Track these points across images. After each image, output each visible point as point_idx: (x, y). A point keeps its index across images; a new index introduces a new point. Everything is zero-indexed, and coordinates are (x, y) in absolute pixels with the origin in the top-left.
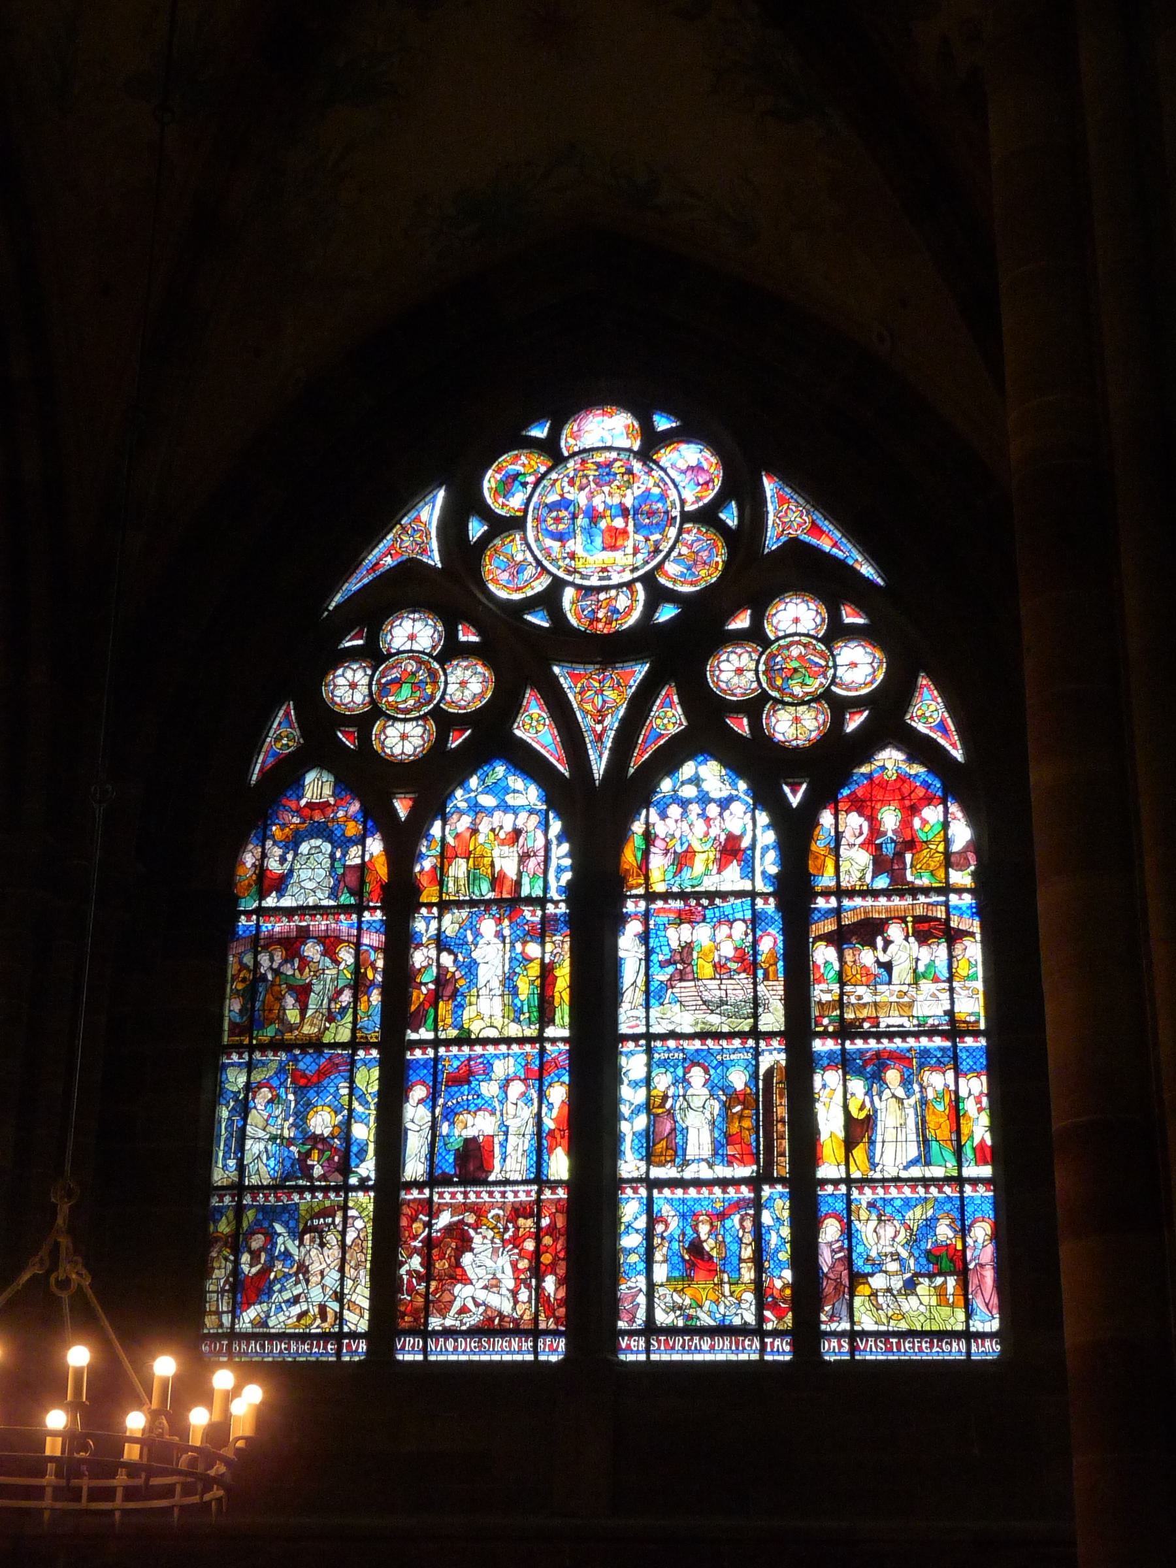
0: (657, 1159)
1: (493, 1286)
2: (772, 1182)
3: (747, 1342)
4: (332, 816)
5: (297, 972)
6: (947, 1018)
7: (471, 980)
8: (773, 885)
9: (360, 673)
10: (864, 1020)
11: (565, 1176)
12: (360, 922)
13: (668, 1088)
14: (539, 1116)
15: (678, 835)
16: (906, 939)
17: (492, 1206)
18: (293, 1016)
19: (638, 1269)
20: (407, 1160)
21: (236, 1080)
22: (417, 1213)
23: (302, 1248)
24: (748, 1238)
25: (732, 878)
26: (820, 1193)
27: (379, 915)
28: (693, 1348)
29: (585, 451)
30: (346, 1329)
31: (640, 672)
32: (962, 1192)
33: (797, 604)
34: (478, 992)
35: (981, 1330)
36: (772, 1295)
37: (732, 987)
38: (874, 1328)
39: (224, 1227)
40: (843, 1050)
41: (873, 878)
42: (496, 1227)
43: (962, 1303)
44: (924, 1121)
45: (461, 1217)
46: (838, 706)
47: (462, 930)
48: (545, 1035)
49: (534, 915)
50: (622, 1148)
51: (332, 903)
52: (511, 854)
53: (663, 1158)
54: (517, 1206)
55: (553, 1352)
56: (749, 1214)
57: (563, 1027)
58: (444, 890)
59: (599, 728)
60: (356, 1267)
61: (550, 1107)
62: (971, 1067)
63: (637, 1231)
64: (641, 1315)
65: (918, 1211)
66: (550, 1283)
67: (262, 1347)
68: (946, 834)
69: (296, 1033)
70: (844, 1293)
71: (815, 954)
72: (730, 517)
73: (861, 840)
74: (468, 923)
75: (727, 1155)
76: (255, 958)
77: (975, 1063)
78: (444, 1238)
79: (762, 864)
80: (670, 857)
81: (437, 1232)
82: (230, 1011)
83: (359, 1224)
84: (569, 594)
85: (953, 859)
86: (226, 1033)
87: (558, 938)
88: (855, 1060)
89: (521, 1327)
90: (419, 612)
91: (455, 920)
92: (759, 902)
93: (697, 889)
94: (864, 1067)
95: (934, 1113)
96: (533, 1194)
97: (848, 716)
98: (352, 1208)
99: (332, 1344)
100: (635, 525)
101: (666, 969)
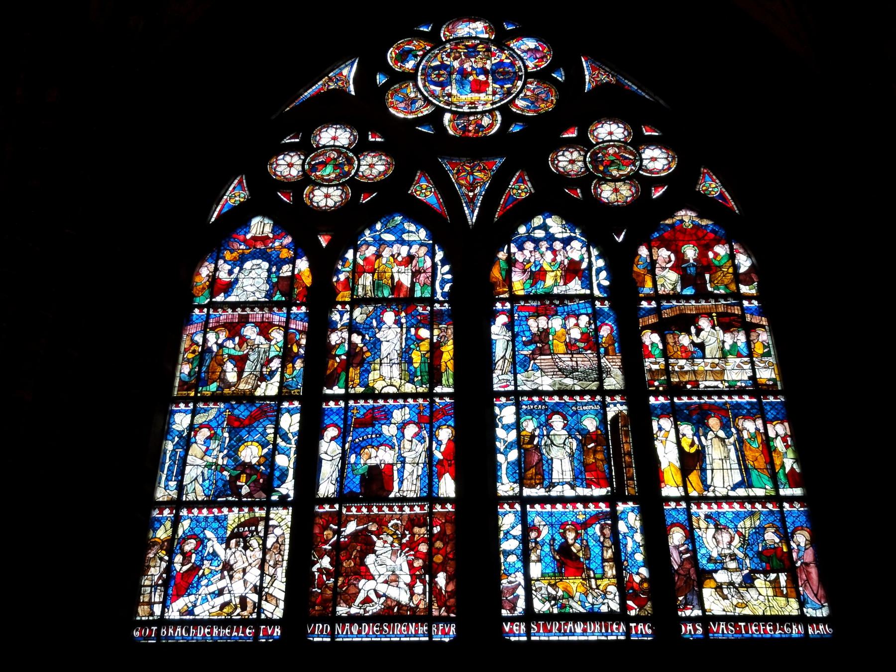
3: (615, 626)
4: (270, 245)
5: (237, 346)
11: (452, 495)
12: (289, 313)
14: (430, 452)
16: (713, 327)
18: (232, 377)
19: (516, 566)
21: (181, 421)
22: (328, 523)
24: (608, 543)
25: (575, 287)
27: (304, 309)
30: (263, 616)
32: (782, 507)
36: (632, 588)
37: (581, 359)
39: (162, 534)
41: (682, 290)
42: (395, 533)
44: (743, 456)
47: (369, 319)
49: (424, 309)
50: (499, 474)
55: (445, 634)
56: (607, 524)
58: (355, 293)
60: (275, 566)
62: (775, 416)
63: (514, 537)
65: (748, 523)
67: (188, 631)
69: (233, 388)
70: (694, 586)
72: (559, 76)
73: (669, 265)
74: (374, 314)
77: (778, 414)
79: (597, 279)
80: (527, 275)
81: (345, 538)
83: (278, 531)
85: (741, 278)
86: (176, 389)
89: (418, 614)
90: (340, 124)
92: (598, 304)
96: (426, 508)
98: (272, 519)
99: (250, 629)
100: (493, 79)
101: (529, 347)
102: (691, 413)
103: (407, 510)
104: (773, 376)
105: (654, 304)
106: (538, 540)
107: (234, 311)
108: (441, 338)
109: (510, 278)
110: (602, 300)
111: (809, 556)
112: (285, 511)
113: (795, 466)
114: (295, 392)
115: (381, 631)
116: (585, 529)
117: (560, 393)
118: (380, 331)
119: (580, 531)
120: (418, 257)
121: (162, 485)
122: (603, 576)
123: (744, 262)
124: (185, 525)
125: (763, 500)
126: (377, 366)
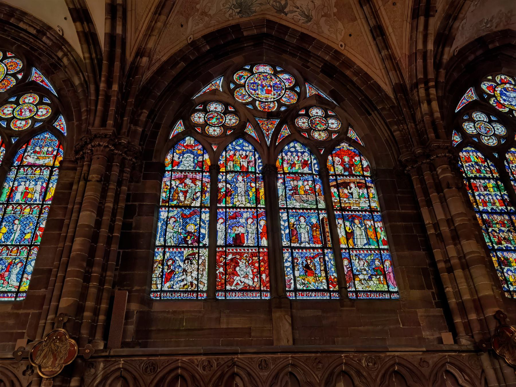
1: (246, 277)
2: (328, 248)
3: (326, 294)
10: (347, 207)
12: (202, 175)
13: (294, 222)
15: (291, 159)
16: (356, 187)
18: (182, 198)
20: (218, 239)
21: (163, 215)
22: (221, 255)
24: (322, 264)
25: (306, 170)
27: (208, 174)
32: (380, 252)
36: (331, 280)
40: (342, 214)
42: (246, 259)
44: (367, 234)
46: (330, 132)
49: (253, 176)
55: (267, 297)
57: (263, 205)
60: (203, 271)
63: (289, 261)
64: (292, 286)
65: (369, 258)
66: (264, 276)
67: (172, 295)
73: (339, 163)
79: (314, 167)
83: (203, 258)
84: (257, 102)
85: (364, 169)
86: (161, 203)
87: (260, 182)
92: (315, 177)
94: (349, 218)
102: (349, 218)
103: (250, 251)
105: (334, 178)
107: (181, 173)
110: (316, 175)
111: (390, 270)
112: (205, 251)
113: (385, 238)
114: (206, 205)
115: (243, 295)
116: (314, 259)
117: (303, 209)
121: (158, 239)
123: (365, 164)
124: (168, 255)
126: (237, 197)
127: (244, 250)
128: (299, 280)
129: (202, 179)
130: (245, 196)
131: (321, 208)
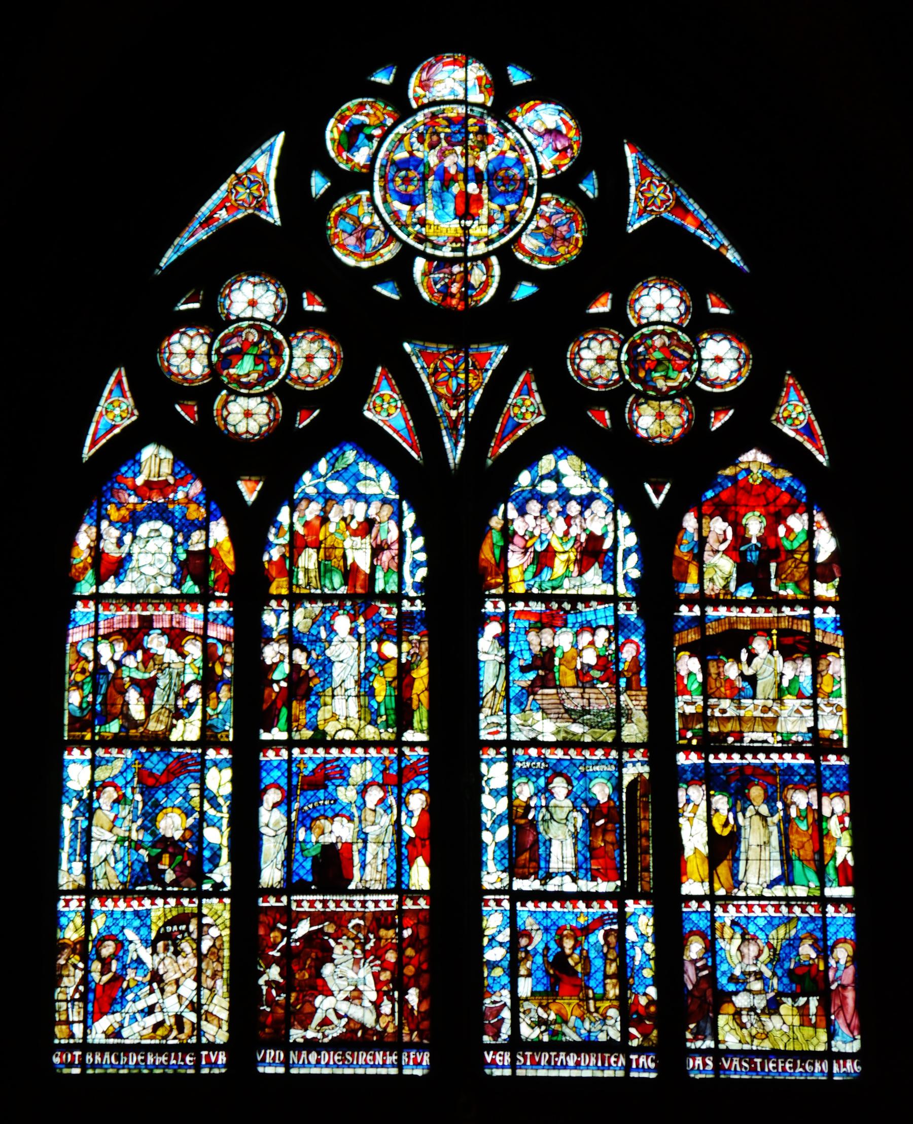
0: (521, 871)
1: (355, 998)
3: (613, 1059)
6: (810, 735)
7: (325, 680)
8: (635, 590)
9: (197, 341)
10: (729, 734)
11: (426, 886)
12: (206, 613)
13: (530, 798)
17: (352, 915)
18: (137, 711)
19: (503, 983)
20: (263, 866)
23: (155, 956)
26: (684, 910)
27: (225, 606)
28: (559, 1064)
29: (434, 103)
30: (204, 1040)
31: (496, 355)
32: (824, 912)
33: (660, 290)
34: (333, 691)
35: (843, 1051)
36: (637, 1012)
38: (737, 1047)
40: (707, 763)
41: (737, 587)
43: (824, 1024)
44: (788, 840)
45: (320, 926)
47: (315, 626)
48: (404, 739)
49: (390, 611)
50: (484, 859)
51: (175, 591)
52: (363, 546)
53: (526, 870)
54: (378, 915)
58: (294, 581)
59: (454, 414)
60: (214, 976)
61: (410, 814)
62: (834, 786)
65: (782, 931)
66: (413, 996)
68: (811, 544)
69: (141, 729)
71: (678, 664)
72: (589, 188)
73: (723, 547)
74: (321, 619)
75: (591, 869)
76: (95, 649)
77: (838, 782)
78: (304, 947)
79: (624, 568)
80: (530, 556)
82: (69, 704)
83: (214, 932)
84: (420, 264)
85: (818, 570)
86: (66, 728)
87: (415, 637)
88: (720, 774)
90: (259, 275)
91: (307, 615)
92: (622, 608)
93: (558, 592)
95: (797, 832)
96: (394, 903)
97: (713, 414)
98: (206, 916)
99: (191, 1056)
100: (489, 192)
104: (840, 727)
105: (697, 611)
106: (529, 948)
108: (412, 657)
109: (506, 561)
111: (848, 976)
116: (587, 938)
118: (330, 645)
119: (580, 939)
120: (380, 523)
122: (604, 997)
125: (803, 902)
127: (351, 903)
128: (530, 1010)
129: (205, 628)
130: (358, 696)
131: (632, 740)
